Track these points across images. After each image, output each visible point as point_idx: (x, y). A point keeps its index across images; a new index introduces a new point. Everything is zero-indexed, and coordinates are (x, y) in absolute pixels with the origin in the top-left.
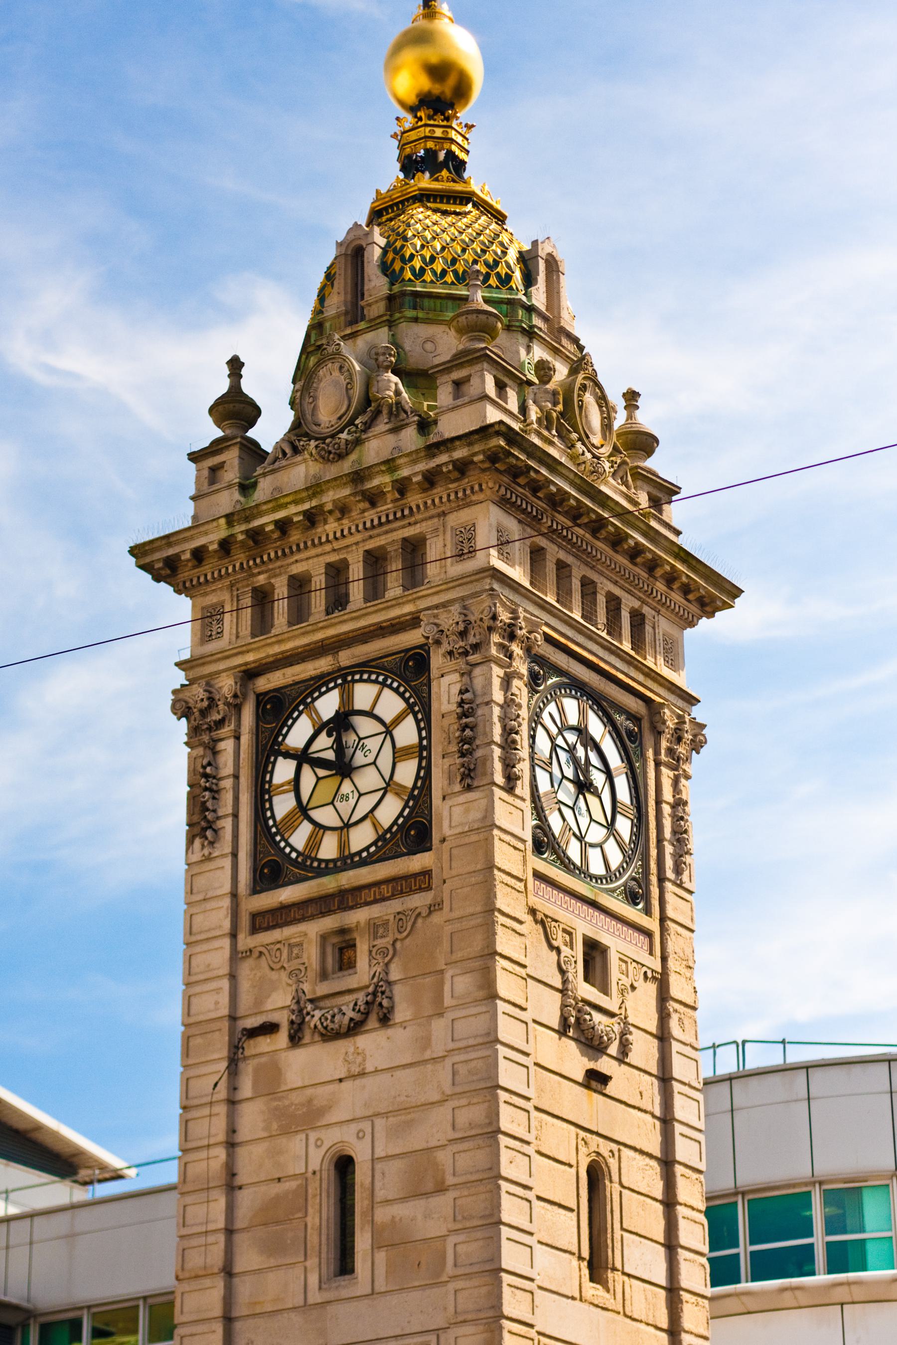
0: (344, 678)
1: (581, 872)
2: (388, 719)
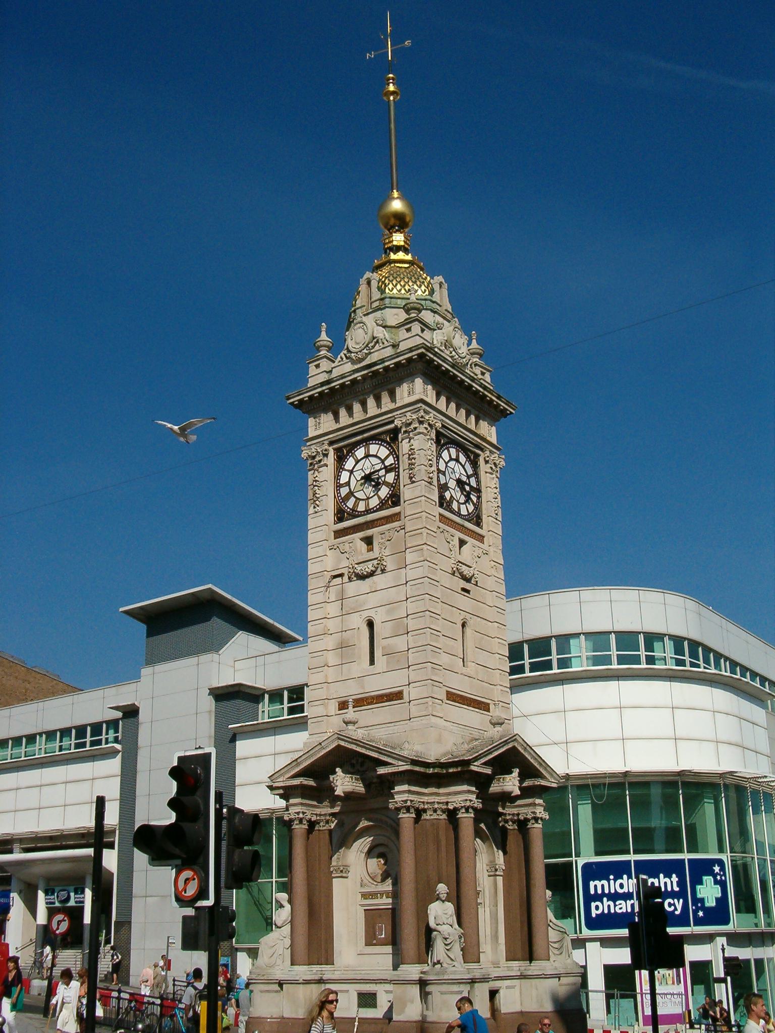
0: (366, 442)
1: (459, 514)
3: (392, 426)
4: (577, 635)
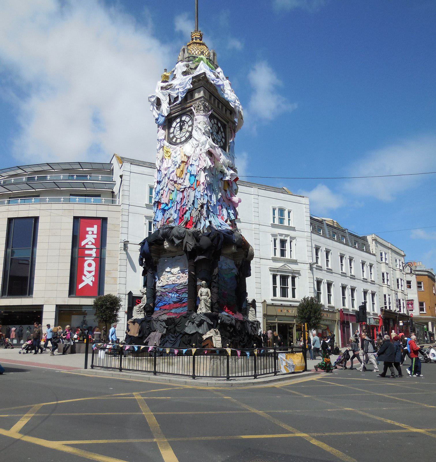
2: (187, 122)
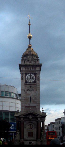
3: (35, 72)
4: (4, 91)
